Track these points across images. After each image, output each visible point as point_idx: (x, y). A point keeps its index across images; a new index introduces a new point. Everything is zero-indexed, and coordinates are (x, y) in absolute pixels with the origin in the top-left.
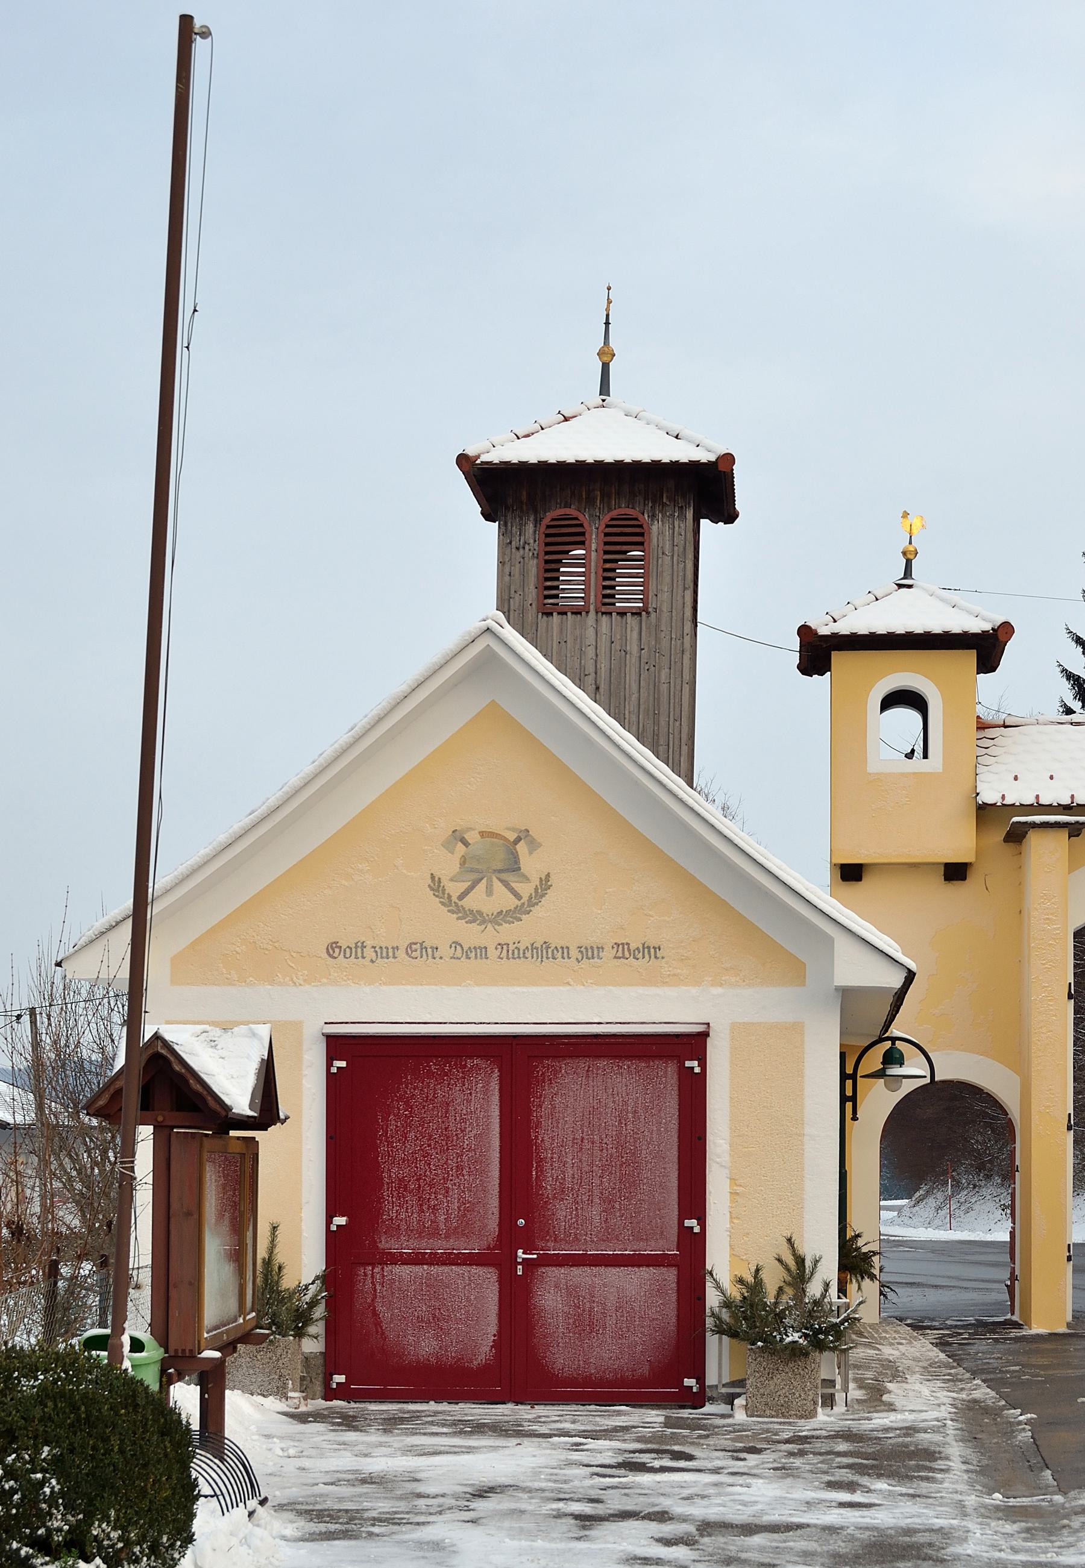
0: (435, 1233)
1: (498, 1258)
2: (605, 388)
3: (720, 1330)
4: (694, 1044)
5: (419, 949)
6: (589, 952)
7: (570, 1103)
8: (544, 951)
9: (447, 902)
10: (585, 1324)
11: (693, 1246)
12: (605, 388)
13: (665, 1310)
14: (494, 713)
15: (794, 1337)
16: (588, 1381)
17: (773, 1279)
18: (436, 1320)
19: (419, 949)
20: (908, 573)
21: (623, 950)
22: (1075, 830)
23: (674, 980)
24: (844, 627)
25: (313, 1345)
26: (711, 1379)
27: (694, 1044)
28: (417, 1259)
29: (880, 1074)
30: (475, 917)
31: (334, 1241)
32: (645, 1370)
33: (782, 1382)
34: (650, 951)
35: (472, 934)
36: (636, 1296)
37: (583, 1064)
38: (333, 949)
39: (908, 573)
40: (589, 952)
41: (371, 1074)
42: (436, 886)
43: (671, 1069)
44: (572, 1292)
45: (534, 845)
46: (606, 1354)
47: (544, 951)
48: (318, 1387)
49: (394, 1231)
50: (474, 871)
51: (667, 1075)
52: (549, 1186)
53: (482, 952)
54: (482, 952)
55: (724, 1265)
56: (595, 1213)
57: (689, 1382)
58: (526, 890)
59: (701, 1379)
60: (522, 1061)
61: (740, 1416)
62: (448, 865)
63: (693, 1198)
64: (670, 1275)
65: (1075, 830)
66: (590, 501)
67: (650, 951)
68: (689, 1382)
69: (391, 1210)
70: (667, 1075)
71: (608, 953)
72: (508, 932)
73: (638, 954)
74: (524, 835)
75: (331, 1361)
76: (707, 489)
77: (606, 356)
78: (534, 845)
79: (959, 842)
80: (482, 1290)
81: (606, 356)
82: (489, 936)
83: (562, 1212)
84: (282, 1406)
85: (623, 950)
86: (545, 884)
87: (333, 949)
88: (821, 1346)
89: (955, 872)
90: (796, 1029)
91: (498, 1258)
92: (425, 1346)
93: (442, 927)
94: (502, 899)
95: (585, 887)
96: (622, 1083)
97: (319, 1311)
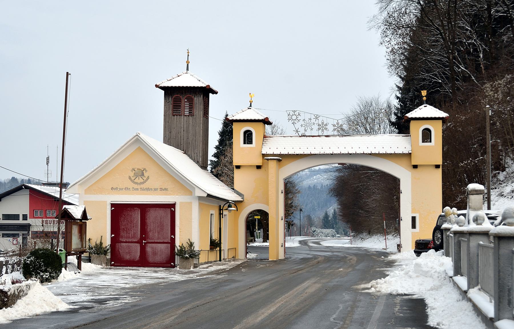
0: (129, 238)
1: (140, 242)
2: (188, 69)
3: (177, 255)
4: (173, 205)
5: (127, 189)
6: (156, 189)
7: (152, 215)
8: (148, 189)
9: (132, 181)
10: (155, 253)
11: (173, 241)
12: (188, 69)
13: (168, 251)
14: (139, 149)
15: (187, 256)
16: (155, 263)
17: (186, 245)
18: (129, 253)
19: (127, 189)
20: (251, 106)
21: (161, 189)
22: (279, 160)
23: (170, 194)
24: (234, 118)
25: (109, 256)
26: (176, 263)
27: (173, 205)
28: (126, 242)
29: (227, 209)
30: (136, 183)
31: (112, 239)
32: (165, 262)
33: (185, 263)
34: (166, 189)
35: (136, 186)
36: (163, 249)
37: (154, 209)
38: (112, 188)
39: (251, 106)
40: (156, 189)
41: (119, 211)
42: (130, 178)
43: (169, 210)
44: (152, 248)
45: (146, 171)
46: (158, 259)
47: (148, 189)
48: (109, 264)
49: (122, 237)
50: (136, 175)
51: (168, 211)
52: (148, 230)
53: (137, 189)
54: (137, 189)
55: (178, 244)
56: (156, 234)
57: (172, 264)
58: (145, 179)
59: (174, 263)
60: (144, 208)
61: (178, 269)
62: (132, 174)
63: (173, 232)
64: (169, 245)
65: (279, 160)
66: (182, 93)
67: (166, 189)
68: (172, 264)
69: (122, 234)
70: (168, 211)
71: (159, 190)
72: (142, 186)
73: (164, 190)
74: (145, 169)
75: (112, 259)
76: (206, 92)
77: (188, 63)
78: (146, 171)
79: (259, 162)
80: (138, 247)
81: (188, 63)
82: (139, 187)
83: (151, 234)
84: (102, 267)
85: (161, 189)
86: (148, 178)
87: (112, 188)
88: (192, 257)
89: (259, 167)
90: (191, 203)
91: (140, 242)
92: (127, 257)
93: (131, 185)
94: (142, 181)
95: (155, 180)
96: (161, 212)
97: (109, 251)
